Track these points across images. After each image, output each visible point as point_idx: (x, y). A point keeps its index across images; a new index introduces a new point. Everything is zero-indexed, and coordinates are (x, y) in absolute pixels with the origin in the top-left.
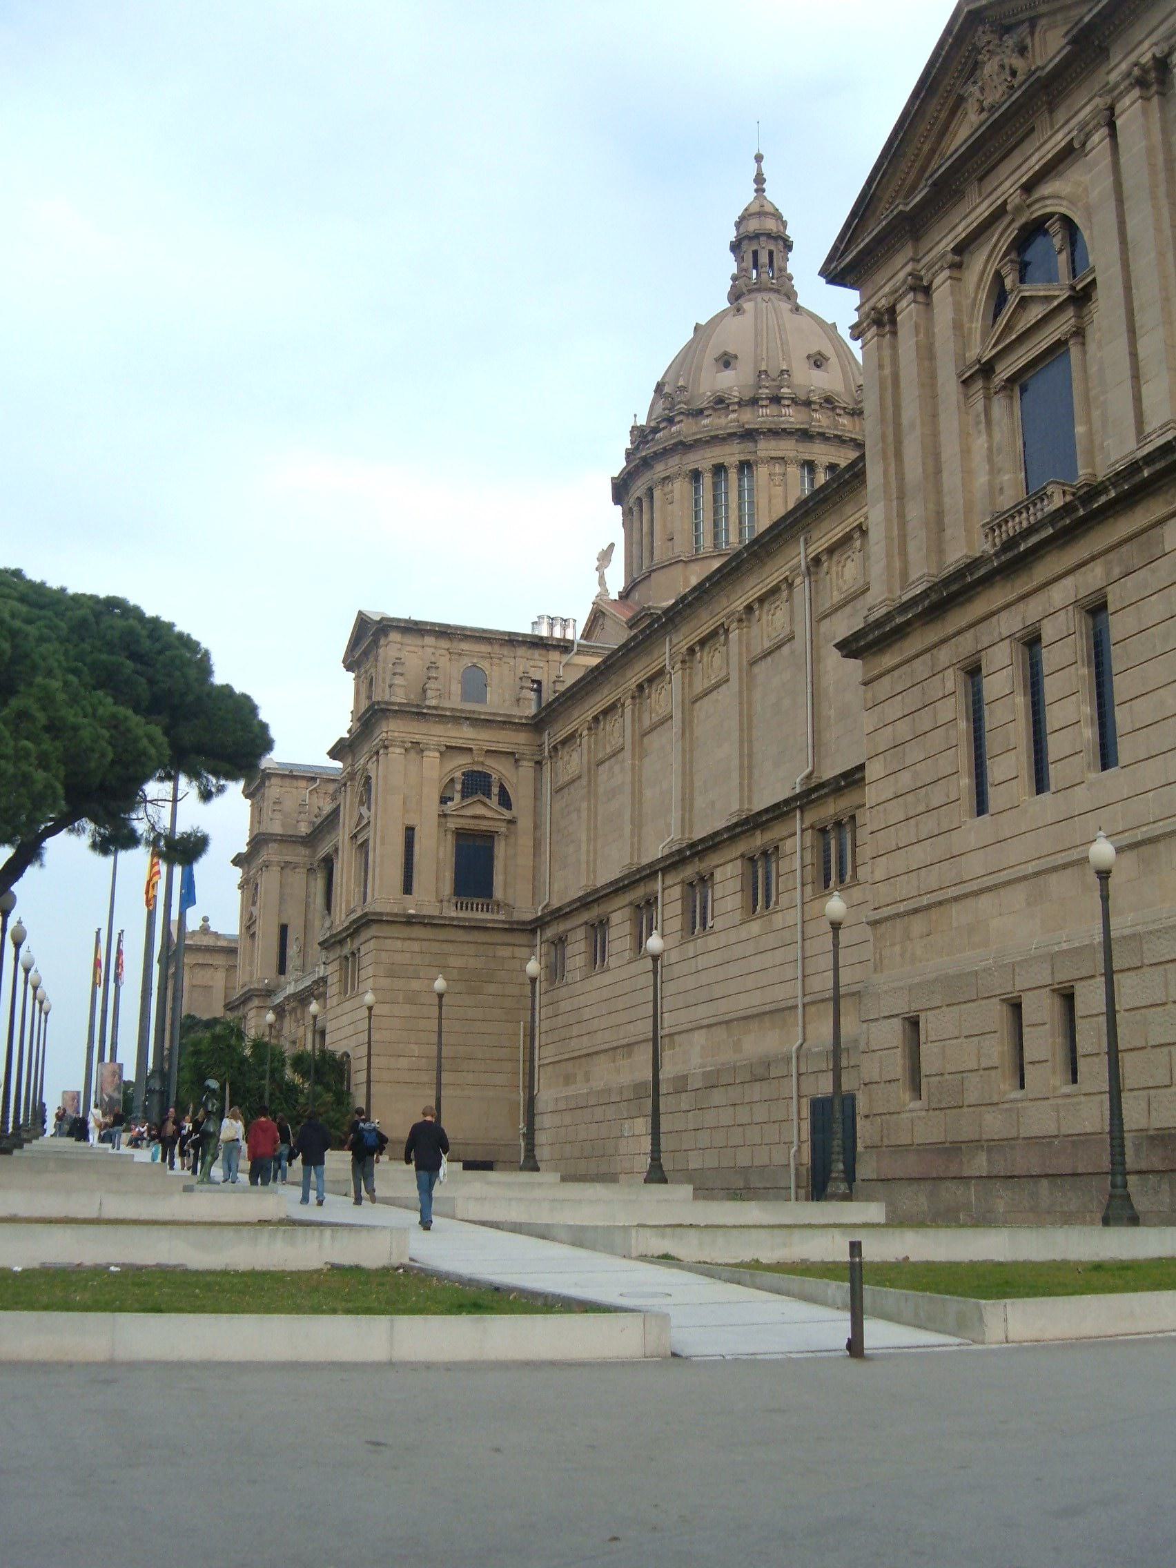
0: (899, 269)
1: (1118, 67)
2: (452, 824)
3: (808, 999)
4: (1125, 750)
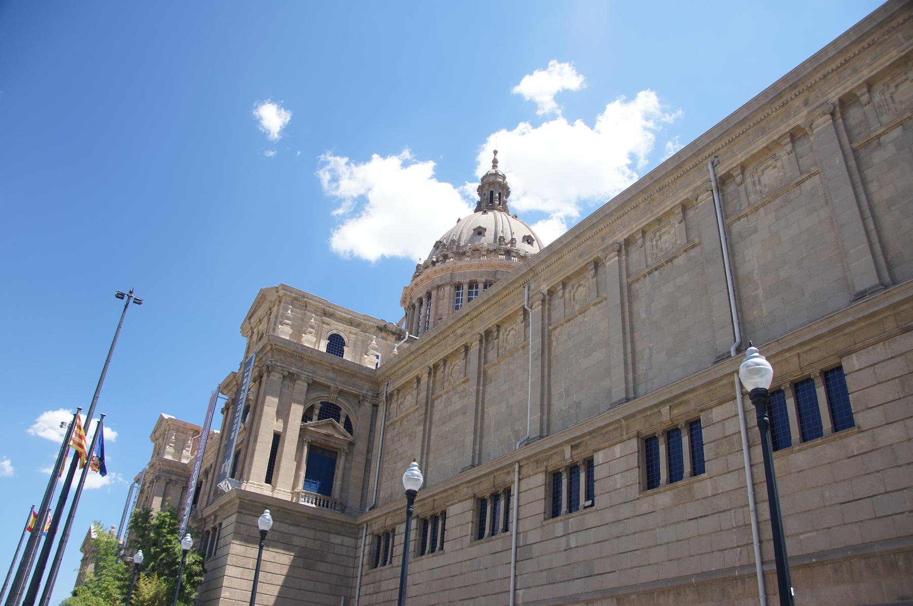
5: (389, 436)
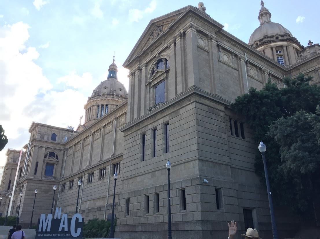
0: (136, 66)
1: (177, 33)
2: (46, 162)
3: (109, 195)
4: (171, 149)
5: (67, 159)
